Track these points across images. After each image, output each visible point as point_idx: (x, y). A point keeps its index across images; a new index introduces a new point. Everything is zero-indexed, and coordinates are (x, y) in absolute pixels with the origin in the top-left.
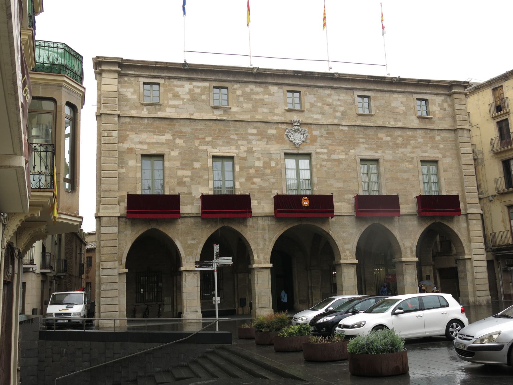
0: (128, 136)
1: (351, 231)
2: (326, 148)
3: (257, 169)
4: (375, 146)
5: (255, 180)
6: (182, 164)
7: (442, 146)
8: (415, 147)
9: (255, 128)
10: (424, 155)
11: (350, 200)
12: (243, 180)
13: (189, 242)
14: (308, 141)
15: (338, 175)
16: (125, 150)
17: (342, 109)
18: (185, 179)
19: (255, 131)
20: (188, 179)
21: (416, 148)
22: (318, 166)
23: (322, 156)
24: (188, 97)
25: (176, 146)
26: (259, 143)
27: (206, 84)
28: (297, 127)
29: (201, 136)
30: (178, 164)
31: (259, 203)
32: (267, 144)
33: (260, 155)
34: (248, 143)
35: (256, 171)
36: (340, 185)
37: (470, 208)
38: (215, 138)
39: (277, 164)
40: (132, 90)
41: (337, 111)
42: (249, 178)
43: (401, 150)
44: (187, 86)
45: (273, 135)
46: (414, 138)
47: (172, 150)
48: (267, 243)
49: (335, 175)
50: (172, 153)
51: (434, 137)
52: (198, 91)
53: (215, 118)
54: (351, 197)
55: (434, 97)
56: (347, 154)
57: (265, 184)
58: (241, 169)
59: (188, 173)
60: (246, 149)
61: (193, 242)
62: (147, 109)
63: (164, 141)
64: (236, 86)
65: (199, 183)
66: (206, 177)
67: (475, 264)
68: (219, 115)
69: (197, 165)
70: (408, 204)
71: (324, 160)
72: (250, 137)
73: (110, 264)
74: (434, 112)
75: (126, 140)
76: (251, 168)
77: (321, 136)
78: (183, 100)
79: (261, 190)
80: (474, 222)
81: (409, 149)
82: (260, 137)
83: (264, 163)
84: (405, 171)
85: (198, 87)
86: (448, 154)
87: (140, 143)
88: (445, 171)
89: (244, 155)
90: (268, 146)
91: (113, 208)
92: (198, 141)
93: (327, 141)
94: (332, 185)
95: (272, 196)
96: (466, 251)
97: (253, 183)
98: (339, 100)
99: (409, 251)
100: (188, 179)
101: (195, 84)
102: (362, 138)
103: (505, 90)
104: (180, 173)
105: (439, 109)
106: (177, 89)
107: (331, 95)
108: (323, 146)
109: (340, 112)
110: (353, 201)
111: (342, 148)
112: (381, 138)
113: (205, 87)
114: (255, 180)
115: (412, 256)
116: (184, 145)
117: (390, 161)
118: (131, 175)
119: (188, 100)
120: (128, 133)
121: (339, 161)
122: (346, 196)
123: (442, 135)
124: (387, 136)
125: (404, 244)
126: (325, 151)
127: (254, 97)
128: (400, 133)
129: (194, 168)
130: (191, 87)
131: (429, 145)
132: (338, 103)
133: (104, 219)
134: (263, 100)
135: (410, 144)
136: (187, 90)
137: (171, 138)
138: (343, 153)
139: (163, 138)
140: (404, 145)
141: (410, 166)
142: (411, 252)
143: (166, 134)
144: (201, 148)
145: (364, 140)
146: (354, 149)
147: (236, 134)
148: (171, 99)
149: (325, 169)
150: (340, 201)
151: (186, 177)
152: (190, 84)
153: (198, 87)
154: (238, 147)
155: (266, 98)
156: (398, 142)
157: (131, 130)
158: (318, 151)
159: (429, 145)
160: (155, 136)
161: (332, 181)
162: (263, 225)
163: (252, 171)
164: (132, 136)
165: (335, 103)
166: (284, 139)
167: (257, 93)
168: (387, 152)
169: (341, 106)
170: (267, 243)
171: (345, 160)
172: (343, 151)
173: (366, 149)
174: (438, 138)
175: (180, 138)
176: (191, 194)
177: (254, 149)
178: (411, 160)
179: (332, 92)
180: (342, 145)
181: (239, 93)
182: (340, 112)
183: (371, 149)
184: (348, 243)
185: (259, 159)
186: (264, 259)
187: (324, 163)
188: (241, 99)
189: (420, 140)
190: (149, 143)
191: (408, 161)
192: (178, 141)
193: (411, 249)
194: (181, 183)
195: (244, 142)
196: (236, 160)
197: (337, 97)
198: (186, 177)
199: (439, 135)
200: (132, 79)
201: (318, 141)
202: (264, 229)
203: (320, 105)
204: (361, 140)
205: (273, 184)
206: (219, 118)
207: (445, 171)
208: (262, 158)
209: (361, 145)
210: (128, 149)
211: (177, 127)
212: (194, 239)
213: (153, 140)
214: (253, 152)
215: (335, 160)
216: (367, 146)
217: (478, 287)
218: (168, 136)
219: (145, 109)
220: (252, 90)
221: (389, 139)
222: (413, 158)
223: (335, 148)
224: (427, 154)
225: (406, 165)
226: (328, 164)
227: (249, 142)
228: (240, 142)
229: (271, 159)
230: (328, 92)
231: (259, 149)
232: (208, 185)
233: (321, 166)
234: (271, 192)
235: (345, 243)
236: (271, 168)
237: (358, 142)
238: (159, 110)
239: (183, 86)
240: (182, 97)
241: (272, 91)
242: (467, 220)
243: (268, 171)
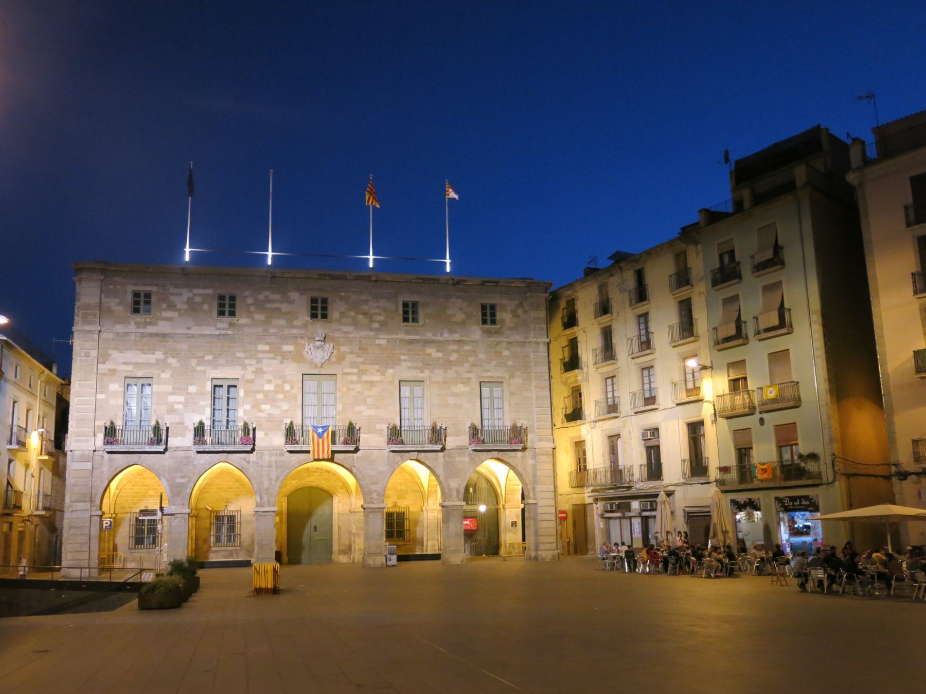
0: (110, 355)
1: (381, 469)
2: (357, 367)
3: (266, 394)
4: (420, 365)
5: (263, 407)
6: (174, 388)
7: (510, 363)
8: (473, 365)
9: (267, 344)
10: (486, 374)
11: (382, 430)
12: (248, 407)
13: (178, 481)
14: (334, 359)
15: (369, 401)
16: (106, 372)
17: (381, 318)
18: (176, 406)
19: (267, 348)
20: (180, 407)
21: (475, 365)
22: (345, 389)
23: (351, 378)
24: (186, 307)
25: (169, 366)
26: (271, 361)
27: (210, 291)
28: (319, 343)
29: (199, 354)
30: (169, 388)
31: (266, 434)
32: (281, 363)
33: (271, 377)
34: (257, 362)
35: (265, 396)
36: (372, 412)
37: (540, 440)
38: (216, 357)
39: (292, 388)
40: (117, 300)
41: (374, 321)
42: (256, 406)
43: (455, 368)
44: (186, 294)
45: (290, 352)
46: (474, 353)
47: (163, 372)
48: (273, 483)
49: (365, 401)
50: (163, 375)
51: (501, 352)
52: (198, 299)
53: (217, 332)
54: (384, 427)
55: (505, 301)
56: (383, 374)
57: (276, 412)
58: (247, 393)
59: (181, 399)
60: (254, 369)
61: (182, 480)
62: (136, 323)
63: (153, 361)
64: (247, 293)
65: (193, 411)
66: (202, 403)
67: (540, 510)
68: (223, 329)
69: (192, 389)
70: (458, 436)
71: (352, 382)
72: (260, 355)
73: (80, 506)
74: (503, 321)
75: (108, 359)
76: (258, 392)
77: (351, 353)
78: (179, 310)
79: (270, 418)
80: (544, 458)
81: (467, 365)
82: (271, 355)
83: (276, 387)
84: (456, 395)
85: (200, 295)
86: (518, 373)
87: (125, 363)
88: (512, 394)
89: (251, 377)
90: (282, 366)
91: (87, 441)
92: (196, 360)
93: (359, 360)
94: (360, 412)
95: (283, 427)
96: (531, 495)
97: (261, 411)
98: (378, 307)
99: (454, 494)
100: (180, 407)
101: (196, 291)
102: (404, 354)
103: (610, 288)
104: (171, 399)
105: (510, 316)
106: (173, 298)
107: (368, 300)
108: (353, 365)
109: (378, 322)
110: (385, 432)
111: (377, 367)
112: (430, 355)
113: (208, 295)
114: (263, 407)
115: (459, 500)
116: (178, 365)
117: (439, 382)
118: (112, 401)
119: (186, 310)
120: (110, 352)
121: (372, 384)
122: (378, 426)
123: (512, 349)
124: (438, 351)
125: (448, 486)
126: (355, 371)
127: (269, 305)
128: (455, 347)
129: (188, 393)
130: (191, 295)
131: (494, 363)
132: (377, 311)
133: (77, 453)
134: (279, 309)
135: (467, 362)
136: (185, 298)
137: (162, 357)
138: (378, 374)
139: (151, 358)
140: (459, 363)
141: (466, 389)
142: (458, 495)
143: (157, 353)
144: (199, 368)
145: (406, 357)
146: (393, 368)
147: (244, 352)
148: (165, 310)
149: (353, 393)
150: (370, 432)
151: (178, 403)
152: (190, 291)
153: (200, 295)
154: (244, 367)
155: (284, 307)
156: (451, 358)
157: (115, 349)
158: (346, 371)
159: (494, 363)
160: (144, 356)
161: (359, 408)
162: (270, 461)
163: (260, 396)
164: (115, 354)
165: (372, 311)
166: (303, 356)
167: (272, 301)
168: (436, 371)
169: (379, 314)
170: (273, 483)
171: (380, 382)
172: (377, 371)
173: (409, 368)
174: (506, 353)
175: (173, 357)
176: (182, 423)
177: (265, 369)
178: (467, 382)
179: (370, 298)
180: (376, 364)
181: (250, 301)
182: (378, 322)
183: (415, 368)
184: (376, 483)
185: (269, 382)
186: (269, 501)
187: (352, 386)
188: (252, 308)
189: (482, 356)
190: (136, 364)
191: (462, 383)
192: (172, 361)
193: (458, 491)
194: (171, 410)
195: (253, 362)
196: (240, 384)
197: (376, 304)
198: (178, 403)
199: (507, 349)
200: (119, 287)
201: (347, 358)
202: (270, 466)
203: (352, 313)
204: (403, 357)
205: (286, 411)
206: (223, 332)
207: (512, 394)
208: (273, 381)
209: (403, 364)
210: (110, 370)
211: (170, 344)
212: (183, 477)
213: (140, 361)
214: (264, 373)
215: (366, 382)
216: (409, 364)
217: (543, 540)
218: (159, 355)
219: (132, 323)
220: (266, 297)
221: (440, 355)
222: (470, 379)
223: (367, 367)
224: (489, 374)
225: (461, 388)
226: (358, 387)
227: (259, 361)
228: (247, 362)
229: (285, 382)
230: (364, 297)
231: (271, 369)
232: (204, 414)
233: (348, 390)
234: (282, 421)
235: (373, 484)
236: (284, 392)
237: (399, 359)
238: (150, 324)
239: (180, 295)
240: (178, 307)
241: (292, 298)
242: (534, 456)
243: (281, 396)
